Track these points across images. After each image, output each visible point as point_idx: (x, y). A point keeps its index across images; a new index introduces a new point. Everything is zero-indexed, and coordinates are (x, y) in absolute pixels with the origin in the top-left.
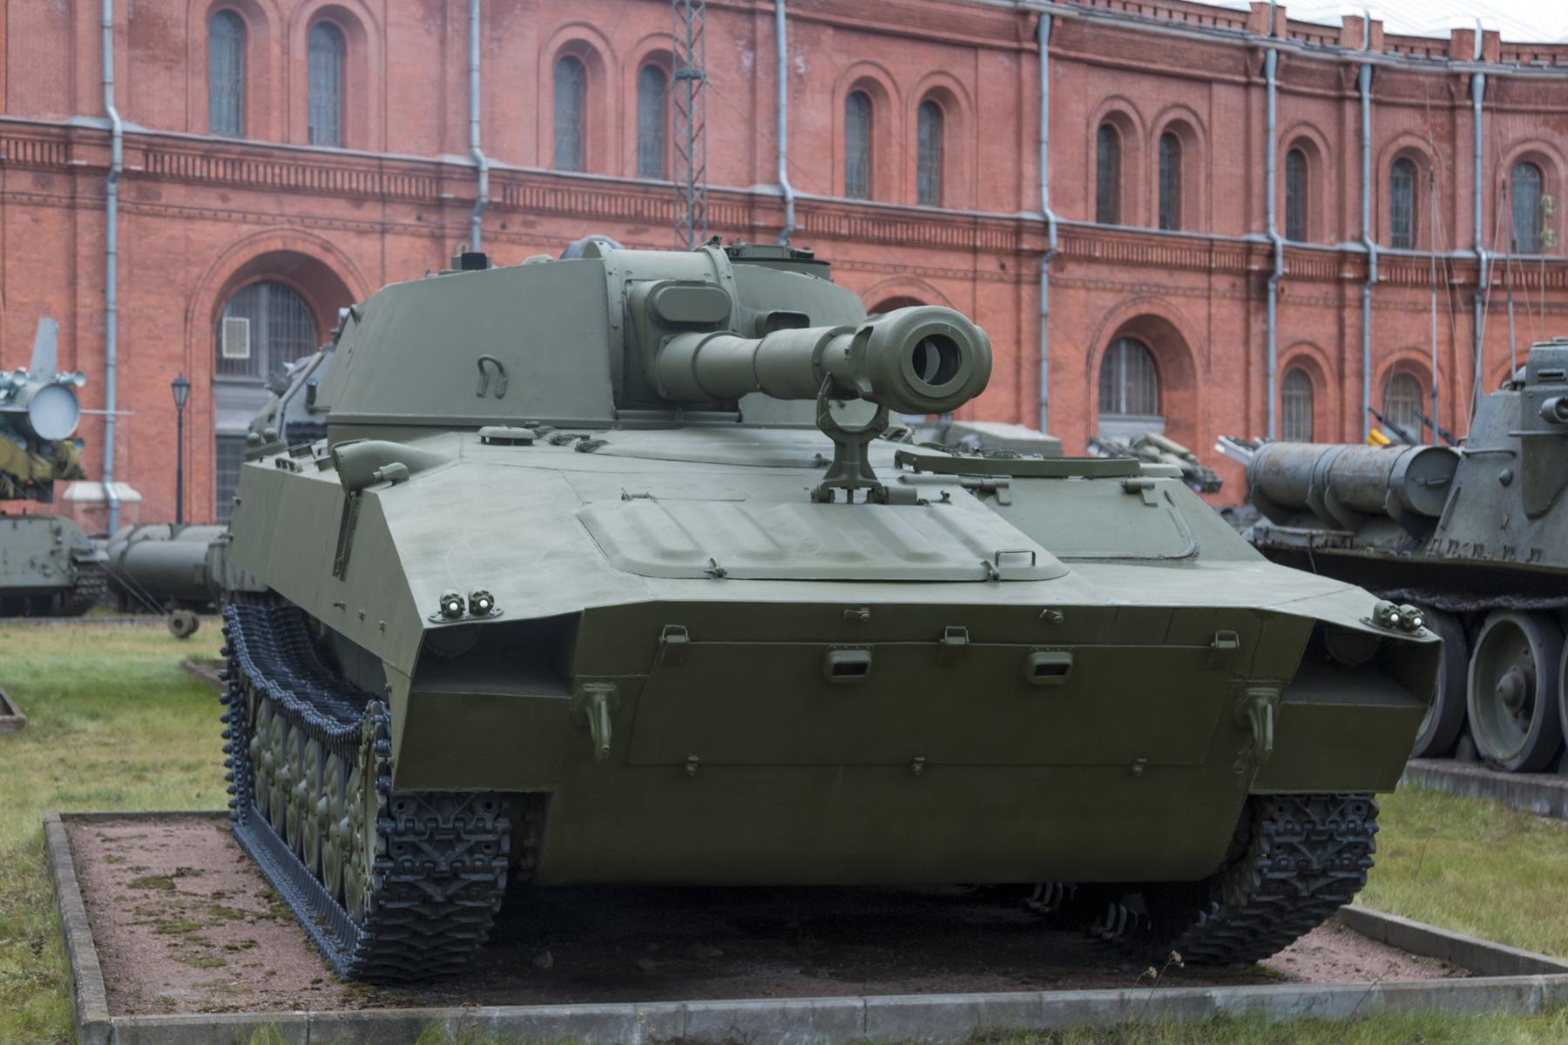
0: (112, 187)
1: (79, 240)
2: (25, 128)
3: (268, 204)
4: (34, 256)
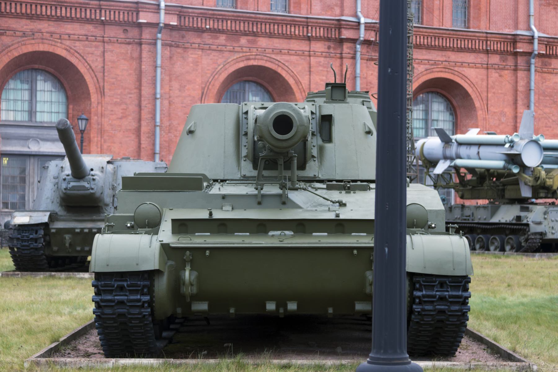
0: (533, 61)
1: (518, 84)
2: (498, 36)
4: (500, 91)
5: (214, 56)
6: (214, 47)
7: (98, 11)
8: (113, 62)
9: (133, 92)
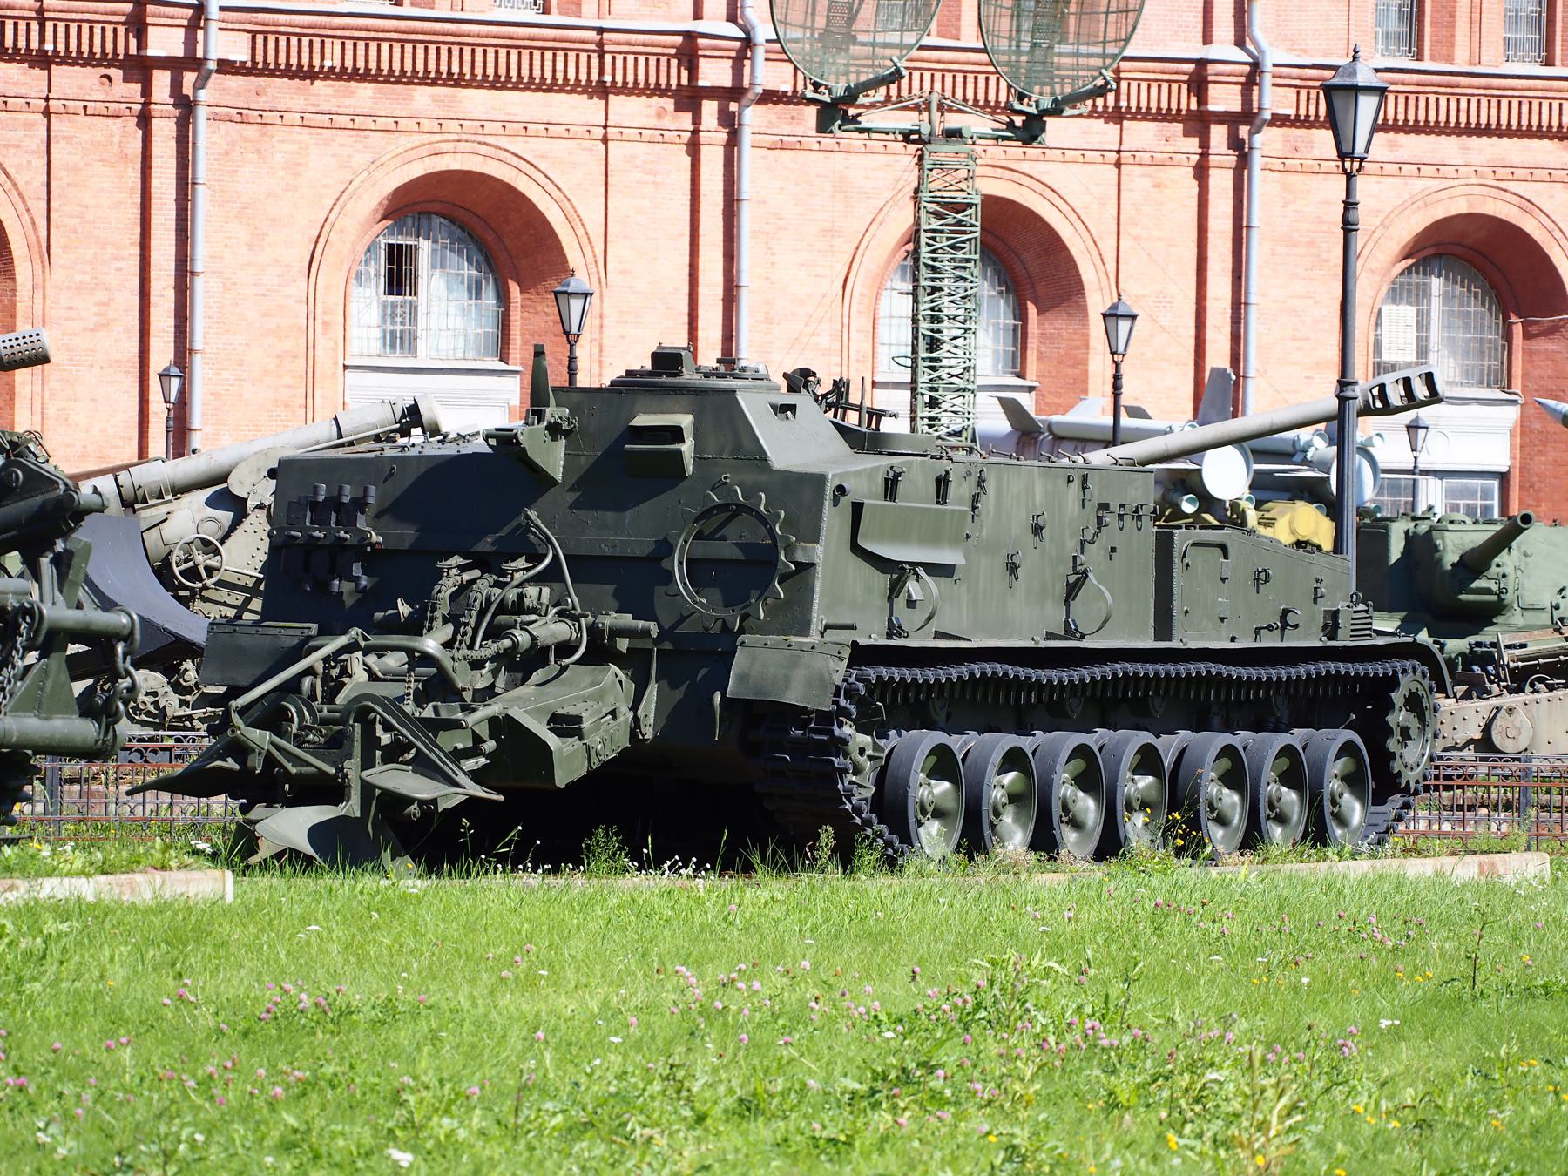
3: (1448, 148)
5: (341, 145)
6: (343, 121)
7: (35, 26)
8: (74, 169)
9: (125, 253)
